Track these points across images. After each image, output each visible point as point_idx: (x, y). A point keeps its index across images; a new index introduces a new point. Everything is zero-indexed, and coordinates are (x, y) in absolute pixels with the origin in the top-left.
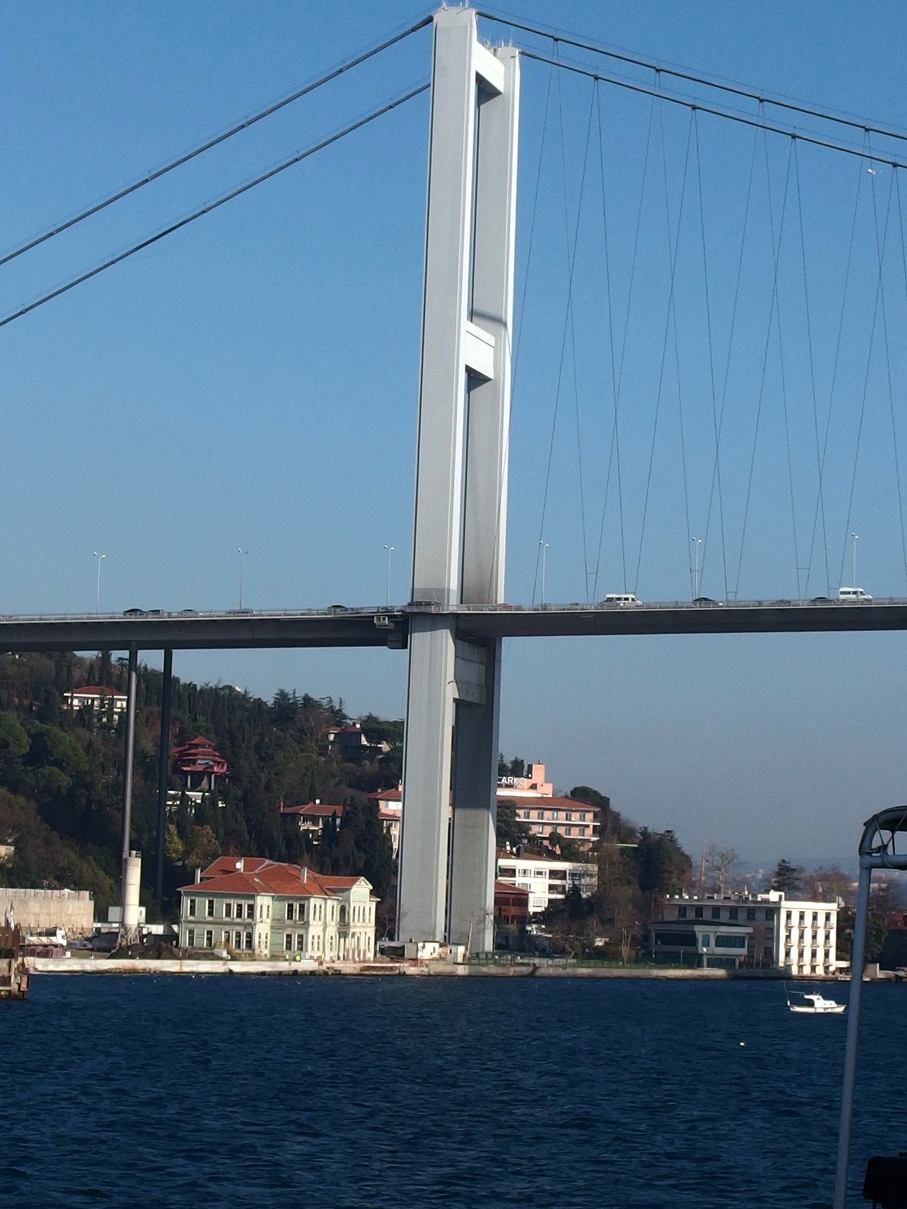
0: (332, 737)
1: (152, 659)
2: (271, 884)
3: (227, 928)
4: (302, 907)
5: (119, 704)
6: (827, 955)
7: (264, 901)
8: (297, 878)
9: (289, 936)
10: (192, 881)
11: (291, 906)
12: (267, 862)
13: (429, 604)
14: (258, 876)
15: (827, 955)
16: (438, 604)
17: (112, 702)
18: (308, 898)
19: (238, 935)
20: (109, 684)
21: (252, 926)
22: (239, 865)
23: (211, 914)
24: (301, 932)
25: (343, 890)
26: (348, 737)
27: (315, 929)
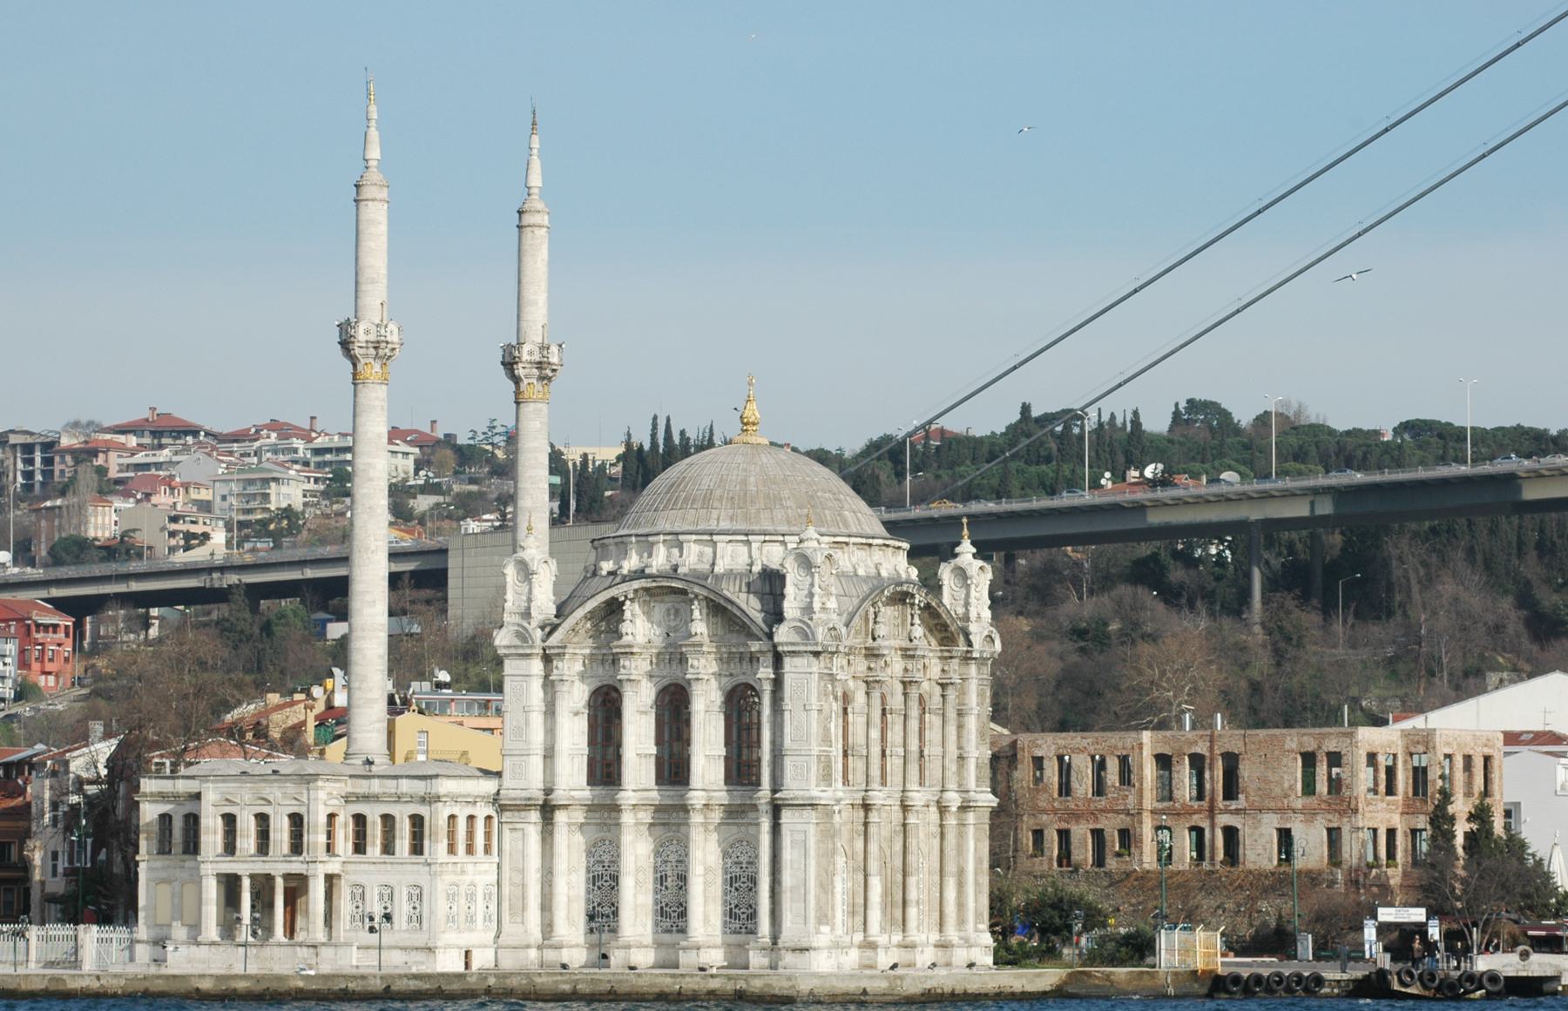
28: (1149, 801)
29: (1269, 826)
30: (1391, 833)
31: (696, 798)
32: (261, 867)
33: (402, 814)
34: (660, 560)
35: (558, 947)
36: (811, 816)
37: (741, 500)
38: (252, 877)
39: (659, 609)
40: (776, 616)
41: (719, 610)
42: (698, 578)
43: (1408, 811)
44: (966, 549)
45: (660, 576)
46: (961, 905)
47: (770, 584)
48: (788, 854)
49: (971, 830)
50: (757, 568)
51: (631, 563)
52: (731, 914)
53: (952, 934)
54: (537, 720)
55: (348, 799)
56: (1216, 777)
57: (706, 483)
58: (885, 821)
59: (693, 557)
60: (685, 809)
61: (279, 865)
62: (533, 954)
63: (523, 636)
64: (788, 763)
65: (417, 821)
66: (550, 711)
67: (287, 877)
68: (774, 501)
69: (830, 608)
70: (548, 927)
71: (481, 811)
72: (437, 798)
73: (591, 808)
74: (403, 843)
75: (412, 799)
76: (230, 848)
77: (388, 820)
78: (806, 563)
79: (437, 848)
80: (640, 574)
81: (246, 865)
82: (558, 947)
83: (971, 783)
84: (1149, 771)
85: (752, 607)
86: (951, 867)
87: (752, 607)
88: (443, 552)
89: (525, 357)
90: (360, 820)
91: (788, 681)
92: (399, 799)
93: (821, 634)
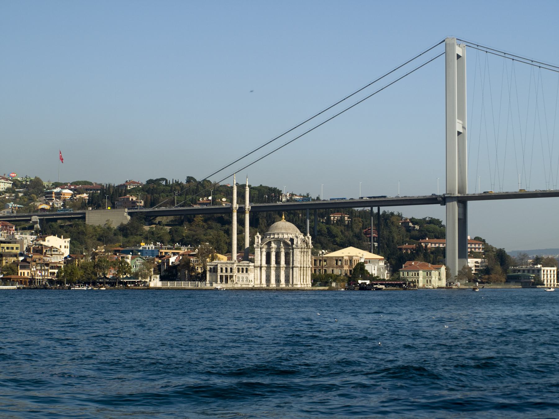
0: (400, 224)
1: (375, 210)
2: (422, 267)
3: (415, 279)
4: (430, 273)
5: (346, 218)
6: (554, 282)
7: (421, 272)
9: (427, 280)
10: (402, 268)
11: (427, 273)
12: (419, 262)
13: (451, 194)
14: (418, 266)
15: (554, 282)
16: (454, 194)
18: (431, 271)
20: (341, 212)
21: (418, 278)
22: (413, 263)
23: (408, 275)
24: (430, 279)
25: (438, 269)
26: (405, 224)
27: (433, 279)
29: (331, 269)
30: (347, 270)
31: (282, 266)
32: (226, 274)
33: (245, 268)
34: (276, 236)
35: (262, 284)
36: (298, 268)
37: (285, 229)
38: (225, 275)
39: (276, 242)
40: (293, 243)
41: (285, 244)
42: (281, 239)
43: (349, 267)
45: (276, 238)
46: (308, 280)
47: (292, 240)
48: (295, 273)
49: (309, 270)
50: (289, 237)
51: (272, 236)
52: (266, 280)
53: (302, 283)
54: (259, 256)
55: (237, 266)
57: (281, 226)
60: (271, 267)
61: (229, 274)
62: (259, 285)
63: (258, 245)
64: (294, 262)
65: (247, 269)
67: (230, 275)
68: (289, 229)
69: (299, 242)
70: (261, 282)
71: (253, 267)
72: (250, 266)
73: (267, 267)
74: (245, 271)
75: (246, 266)
76: (222, 271)
77: (243, 269)
78: (297, 237)
79: (249, 272)
80: (274, 238)
81: (224, 274)
82: (262, 284)
83: (310, 264)
85: (290, 243)
86: (307, 275)
87: (290, 243)
88: (85, 213)
89: (247, 208)
90: (238, 269)
91: (295, 252)
92: (244, 266)
93: (299, 246)
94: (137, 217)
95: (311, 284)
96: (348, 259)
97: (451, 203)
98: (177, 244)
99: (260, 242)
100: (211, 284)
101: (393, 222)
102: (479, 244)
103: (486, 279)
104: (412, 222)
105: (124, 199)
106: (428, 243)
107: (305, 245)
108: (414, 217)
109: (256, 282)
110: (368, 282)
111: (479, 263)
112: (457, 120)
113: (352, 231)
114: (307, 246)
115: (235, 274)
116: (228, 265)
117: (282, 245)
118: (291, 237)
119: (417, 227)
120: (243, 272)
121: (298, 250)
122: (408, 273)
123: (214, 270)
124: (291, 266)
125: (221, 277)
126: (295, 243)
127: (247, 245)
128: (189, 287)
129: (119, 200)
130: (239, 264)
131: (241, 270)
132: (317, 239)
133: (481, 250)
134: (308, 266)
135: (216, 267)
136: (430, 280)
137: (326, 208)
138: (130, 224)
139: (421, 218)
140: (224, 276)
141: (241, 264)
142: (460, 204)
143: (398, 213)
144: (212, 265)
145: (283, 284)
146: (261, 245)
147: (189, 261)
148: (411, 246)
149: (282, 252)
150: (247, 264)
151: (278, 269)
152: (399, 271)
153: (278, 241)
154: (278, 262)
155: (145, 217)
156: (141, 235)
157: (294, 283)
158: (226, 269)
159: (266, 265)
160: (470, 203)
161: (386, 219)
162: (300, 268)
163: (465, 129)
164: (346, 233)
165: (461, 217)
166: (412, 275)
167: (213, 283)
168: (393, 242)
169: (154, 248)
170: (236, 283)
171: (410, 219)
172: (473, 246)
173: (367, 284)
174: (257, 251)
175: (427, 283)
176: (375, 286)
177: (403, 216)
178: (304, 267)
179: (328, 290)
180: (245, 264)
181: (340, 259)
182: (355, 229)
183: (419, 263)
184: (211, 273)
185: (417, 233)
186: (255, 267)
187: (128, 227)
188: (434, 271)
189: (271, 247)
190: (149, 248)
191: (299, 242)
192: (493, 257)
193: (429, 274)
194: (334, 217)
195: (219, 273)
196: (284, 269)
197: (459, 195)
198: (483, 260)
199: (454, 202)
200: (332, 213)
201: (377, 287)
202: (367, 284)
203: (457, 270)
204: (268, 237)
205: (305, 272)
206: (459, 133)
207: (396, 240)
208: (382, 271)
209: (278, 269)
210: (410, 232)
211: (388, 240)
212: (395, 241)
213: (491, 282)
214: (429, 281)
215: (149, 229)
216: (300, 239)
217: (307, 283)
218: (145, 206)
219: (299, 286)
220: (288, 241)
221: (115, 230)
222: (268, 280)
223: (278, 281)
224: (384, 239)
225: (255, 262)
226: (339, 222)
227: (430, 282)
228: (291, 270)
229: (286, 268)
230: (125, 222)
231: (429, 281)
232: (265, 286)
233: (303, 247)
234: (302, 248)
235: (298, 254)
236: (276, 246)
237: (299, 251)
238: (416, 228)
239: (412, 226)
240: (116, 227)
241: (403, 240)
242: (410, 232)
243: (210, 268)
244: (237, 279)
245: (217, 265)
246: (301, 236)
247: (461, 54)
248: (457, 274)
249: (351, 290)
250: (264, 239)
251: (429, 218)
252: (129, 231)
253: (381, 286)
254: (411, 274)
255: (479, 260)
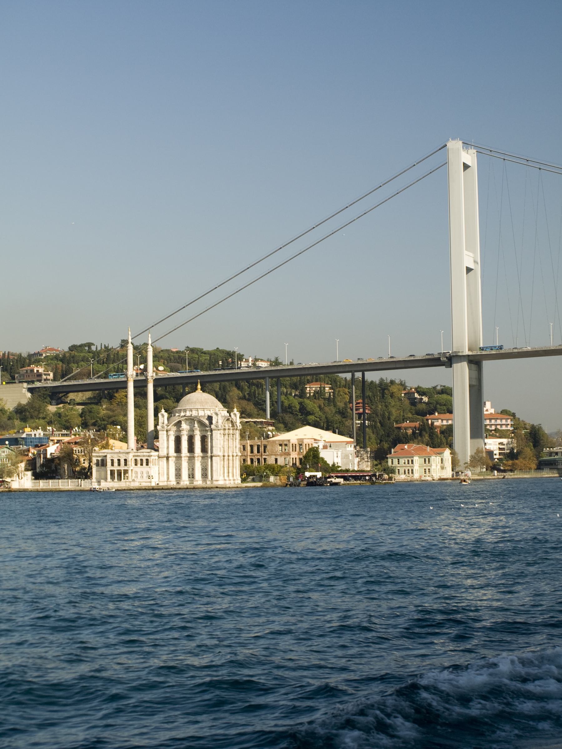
0: (403, 395)
2: (418, 452)
4: (429, 459)
5: (327, 389)
7: (416, 459)
8: (425, 450)
9: (425, 469)
10: (391, 453)
11: (425, 459)
12: (415, 445)
16: (462, 352)
17: (324, 388)
19: (408, 470)
20: (320, 381)
22: (406, 447)
23: (399, 463)
24: (429, 468)
26: (409, 395)
27: (433, 467)
28: (249, 454)
31: (196, 455)
32: (119, 468)
34: (188, 414)
36: (218, 457)
39: (188, 422)
40: (211, 423)
41: (201, 423)
42: (196, 417)
43: (299, 454)
44: (235, 410)
47: (210, 418)
49: (237, 460)
50: (206, 415)
51: (182, 414)
55: (134, 456)
56: (262, 449)
58: (226, 458)
59: (194, 413)
61: (122, 468)
63: (163, 427)
64: (214, 449)
65: (147, 460)
66: (168, 440)
68: (207, 403)
69: (220, 421)
70: (168, 478)
71: (157, 458)
75: (146, 456)
76: (112, 465)
77: (142, 460)
78: (217, 414)
80: (185, 416)
81: (116, 468)
84: (249, 448)
86: (234, 466)
87: (207, 422)
90: (136, 460)
92: (144, 456)
93: (220, 427)
94: (40, 394)
95: (240, 479)
96: (297, 443)
97: (459, 364)
98: (76, 428)
99: (166, 422)
100: (99, 482)
101: (392, 393)
102: (507, 419)
103: (509, 466)
104: (418, 392)
105: (27, 371)
106: (438, 419)
107: (230, 425)
108: (420, 386)
109: (161, 479)
110: (319, 475)
111: (504, 445)
112: (465, 252)
113: (335, 406)
114: (233, 426)
115: (132, 468)
116: (121, 455)
117: (196, 425)
118: (210, 415)
119: (425, 399)
120: (142, 465)
121: (219, 432)
122: (398, 460)
123: (102, 463)
124: (209, 454)
125: (112, 472)
126: (214, 421)
127: (151, 427)
128: (70, 487)
129: (21, 372)
130: (137, 454)
131: (139, 462)
132: (280, 418)
133: (509, 428)
134: (235, 454)
135: (104, 458)
136: (429, 469)
137: (300, 376)
138: (30, 404)
139: (430, 387)
140: (116, 471)
141: (139, 454)
142: (473, 365)
143: (400, 380)
144: (100, 456)
145: (199, 481)
146: (168, 426)
147: (71, 452)
148: (413, 424)
149: (196, 436)
150: (148, 454)
151: (191, 459)
152: (387, 458)
153: (191, 420)
154: (191, 449)
155: (50, 394)
156: (44, 418)
157: (214, 479)
158: (119, 460)
159: (175, 455)
160: (486, 365)
161: (383, 390)
162: (222, 458)
163: (478, 263)
164: (327, 409)
165: (474, 383)
166: (405, 463)
167: (102, 481)
168: (389, 419)
169: (42, 434)
170: (134, 480)
171: (416, 389)
172: (499, 422)
173: (318, 477)
174: (162, 435)
175: (425, 473)
176: (329, 480)
177: (407, 384)
178: (228, 456)
179: (261, 486)
180: (145, 454)
181: (285, 443)
182: (338, 404)
183: (414, 446)
184: (98, 467)
185: (424, 406)
186: (159, 457)
187: (26, 407)
188: (434, 457)
189: (181, 429)
190: (35, 435)
191: (220, 421)
192: (523, 436)
193: (427, 461)
194: (311, 388)
195: (109, 467)
196: (200, 458)
197: (470, 353)
198: (510, 440)
199: (462, 363)
200: (309, 382)
201: (331, 481)
202: (318, 477)
203: (469, 454)
204: (177, 414)
205: (231, 462)
206: (469, 270)
207: (394, 417)
208: (350, 458)
209: (191, 459)
210: (415, 406)
211: (383, 416)
212: (392, 418)
213: (516, 469)
214: (427, 471)
215: (56, 409)
216: (222, 416)
217: (235, 478)
218: (55, 379)
219: (221, 483)
220: (204, 420)
221: (11, 413)
222: (178, 475)
223: (192, 476)
224: (377, 416)
225: (160, 450)
226: (317, 395)
227: (429, 471)
228: (210, 460)
229: (203, 457)
230: (24, 402)
231: (427, 471)
232: (175, 483)
233: (227, 427)
234: (224, 429)
235: (219, 438)
236: (188, 427)
237: (220, 434)
238: (424, 400)
239: (419, 397)
240: (11, 409)
241: (404, 416)
242: (415, 406)
243: (97, 460)
244: (134, 475)
245: (106, 456)
246: (225, 413)
247: (469, 163)
248: (469, 458)
249: (295, 486)
250: (172, 418)
251: (441, 386)
252: (28, 414)
253: (338, 480)
254: (403, 462)
255: (505, 441)
